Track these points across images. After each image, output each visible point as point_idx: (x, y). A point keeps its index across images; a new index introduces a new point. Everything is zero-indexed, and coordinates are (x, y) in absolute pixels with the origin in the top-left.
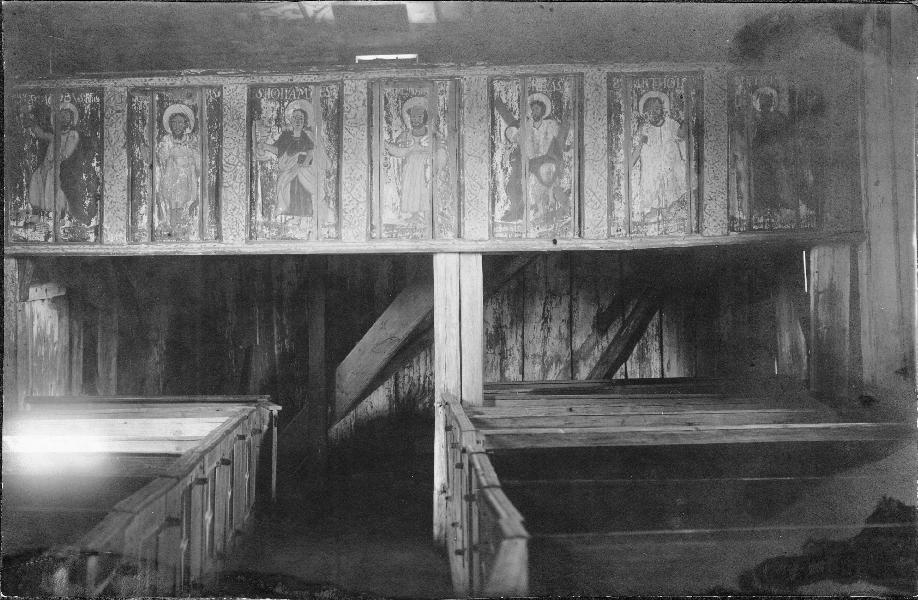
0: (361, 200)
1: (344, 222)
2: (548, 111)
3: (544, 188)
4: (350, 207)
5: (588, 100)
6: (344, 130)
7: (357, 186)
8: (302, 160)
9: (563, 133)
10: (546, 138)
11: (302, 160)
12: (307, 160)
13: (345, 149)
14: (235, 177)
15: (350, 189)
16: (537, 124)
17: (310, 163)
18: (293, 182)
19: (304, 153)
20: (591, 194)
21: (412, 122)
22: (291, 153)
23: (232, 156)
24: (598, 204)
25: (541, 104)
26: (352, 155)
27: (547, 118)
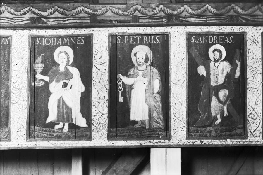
0: (104, 112)
1: (93, 127)
2: (224, 55)
3: (221, 105)
4: (97, 117)
5: (249, 49)
6: (94, 66)
7: (101, 104)
8: (65, 85)
9: (233, 70)
10: (222, 73)
11: (65, 85)
12: (69, 86)
13: (93, 79)
14: (20, 97)
15: (96, 106)
16: (217, 64)
17: (71, 88)
18: (59, 101)
19: (67, 81)
20: (252, 110)
21: (137, 62)
22: (58, 81)
23: (17, 83)
24: (256, 116)
25: (219, 51)
26: (98, 83)
27: (223, 61)
